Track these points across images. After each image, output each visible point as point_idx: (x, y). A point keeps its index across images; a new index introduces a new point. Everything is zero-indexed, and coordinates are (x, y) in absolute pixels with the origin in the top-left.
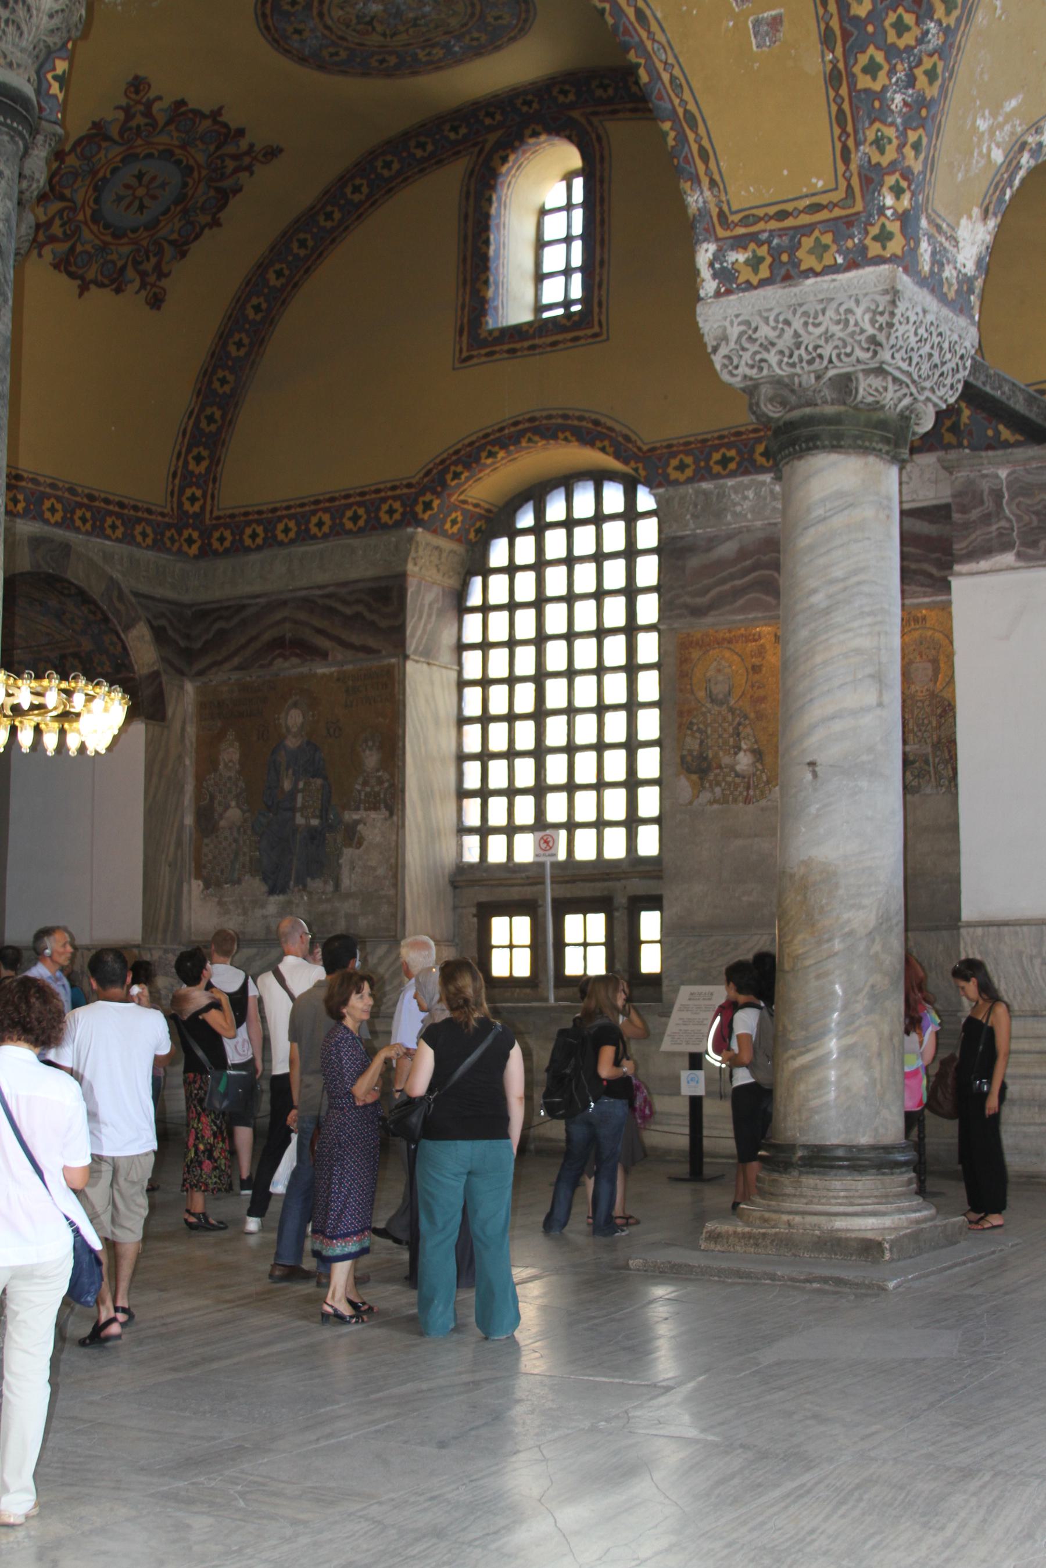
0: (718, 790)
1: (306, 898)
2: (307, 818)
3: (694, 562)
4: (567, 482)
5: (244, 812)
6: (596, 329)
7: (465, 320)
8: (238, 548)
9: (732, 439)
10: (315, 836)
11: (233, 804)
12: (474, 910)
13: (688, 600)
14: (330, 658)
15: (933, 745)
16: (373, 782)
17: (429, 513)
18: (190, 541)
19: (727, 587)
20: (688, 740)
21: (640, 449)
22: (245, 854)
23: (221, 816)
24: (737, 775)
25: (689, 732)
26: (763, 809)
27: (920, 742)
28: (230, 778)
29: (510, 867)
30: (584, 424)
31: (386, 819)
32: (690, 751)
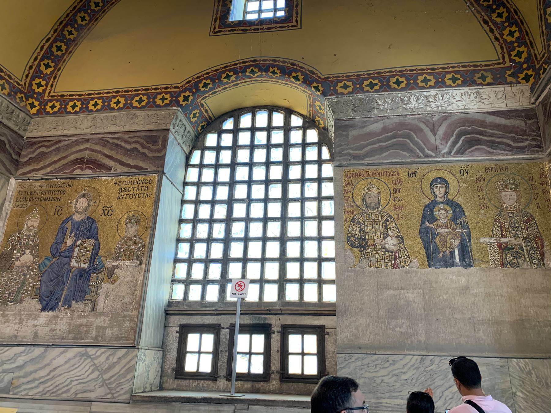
0: (373, 259)
1: (69, 314)
2: (80, 263)
3: (353, 133)
4: (253, 110)
5: (34, 257)
6: (295, 23)
7: (218, 16)
8: (63, 111)
9: (376, 75)
10: (83, 274)
11: (28, 252)
12: (178, 329)
13: (351, 151)
14: (112, 171)
15: (524, 239)
16: (130, 243)
17: (186, 102)
18: (32, 106)
19: (376, 146)
20: (352, 228)
21: (320, 77)
22: (29, 284)
23: (17, 259)
24: (387, 251)
25: (352, 223)
26: (406, 272)
27: (515, 236)
28: (29, 236)
29: (202, 302)
30: (286, 64)
31: (136, 267)
32: (353, 235)
